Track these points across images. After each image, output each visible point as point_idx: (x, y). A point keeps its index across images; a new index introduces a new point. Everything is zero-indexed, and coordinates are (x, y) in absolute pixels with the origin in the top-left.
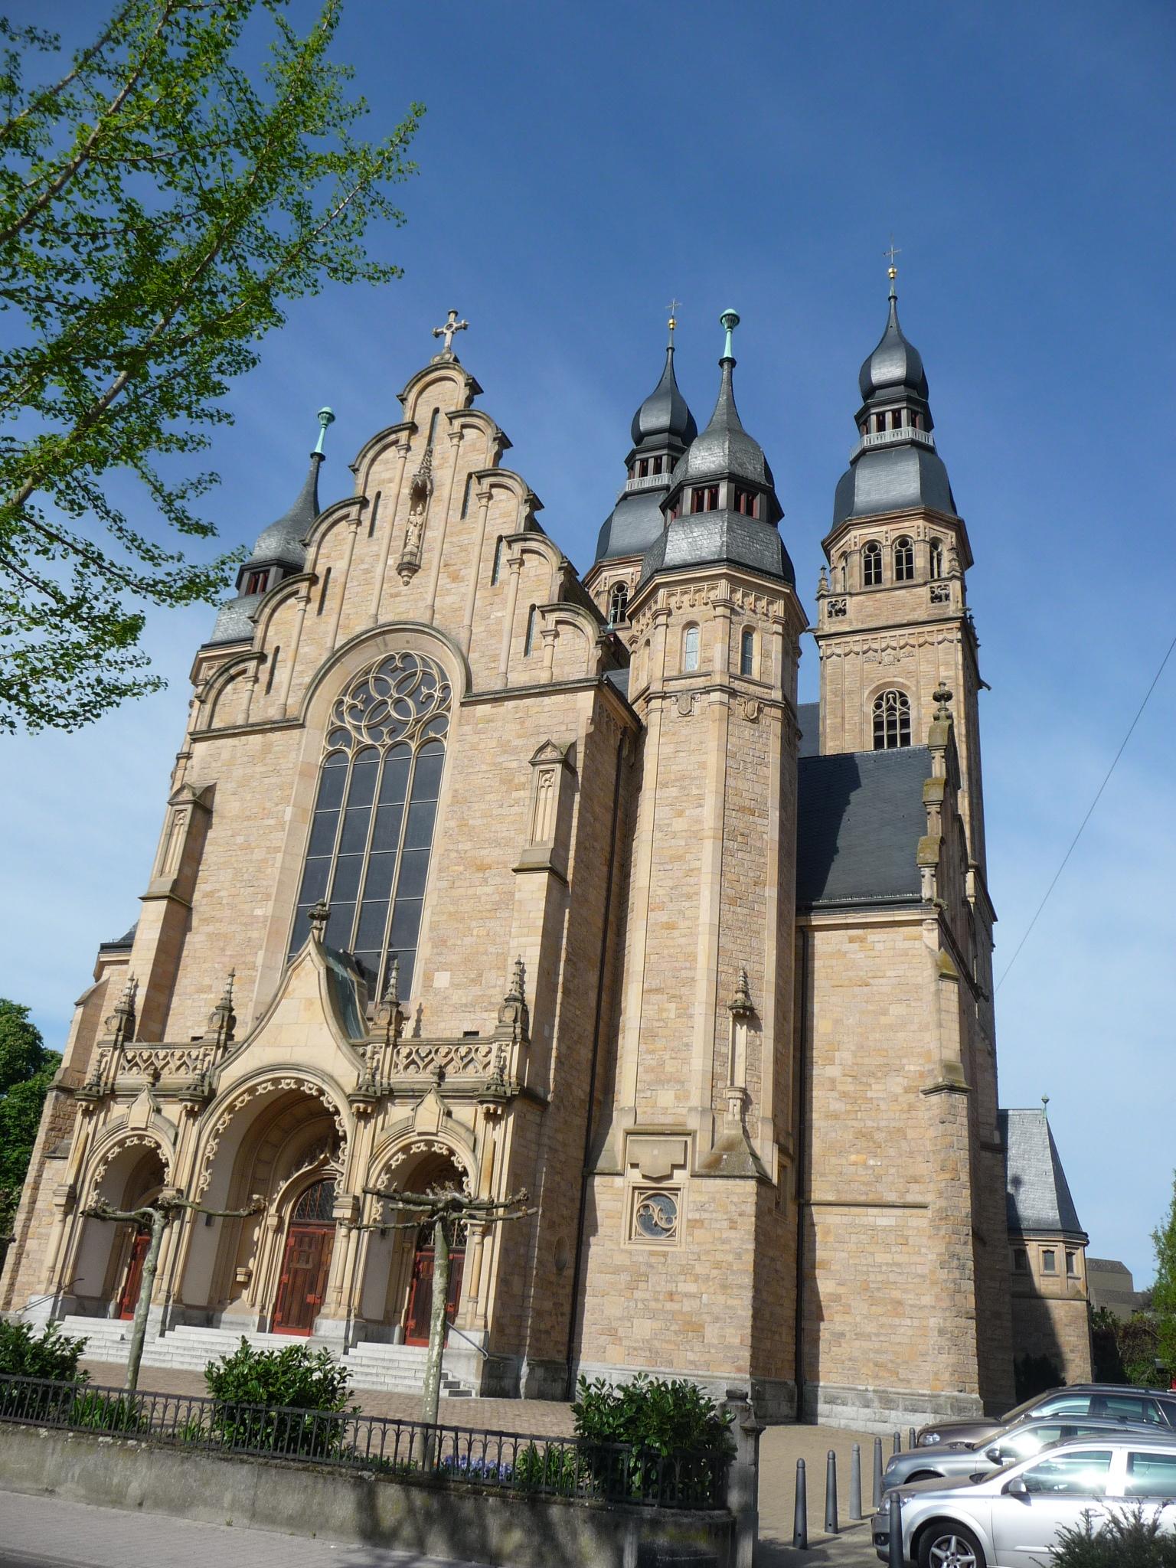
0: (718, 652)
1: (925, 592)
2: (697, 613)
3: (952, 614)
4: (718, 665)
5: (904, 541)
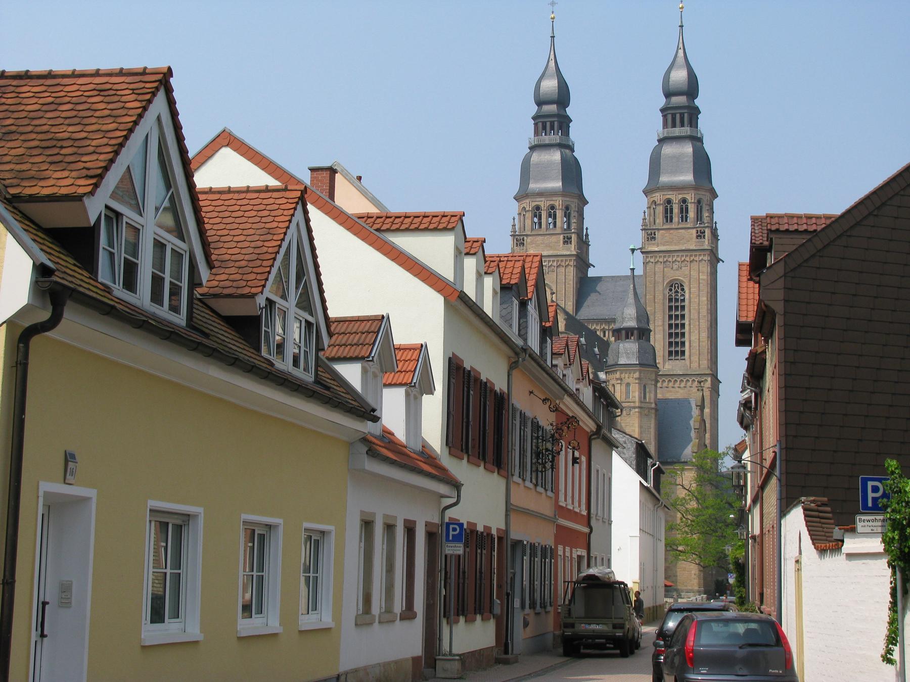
0: (637, 394)
1: (694, 231)
2: (630, 380)
3: (706, 247)
4: (637, 399)
5: (684, 201)
